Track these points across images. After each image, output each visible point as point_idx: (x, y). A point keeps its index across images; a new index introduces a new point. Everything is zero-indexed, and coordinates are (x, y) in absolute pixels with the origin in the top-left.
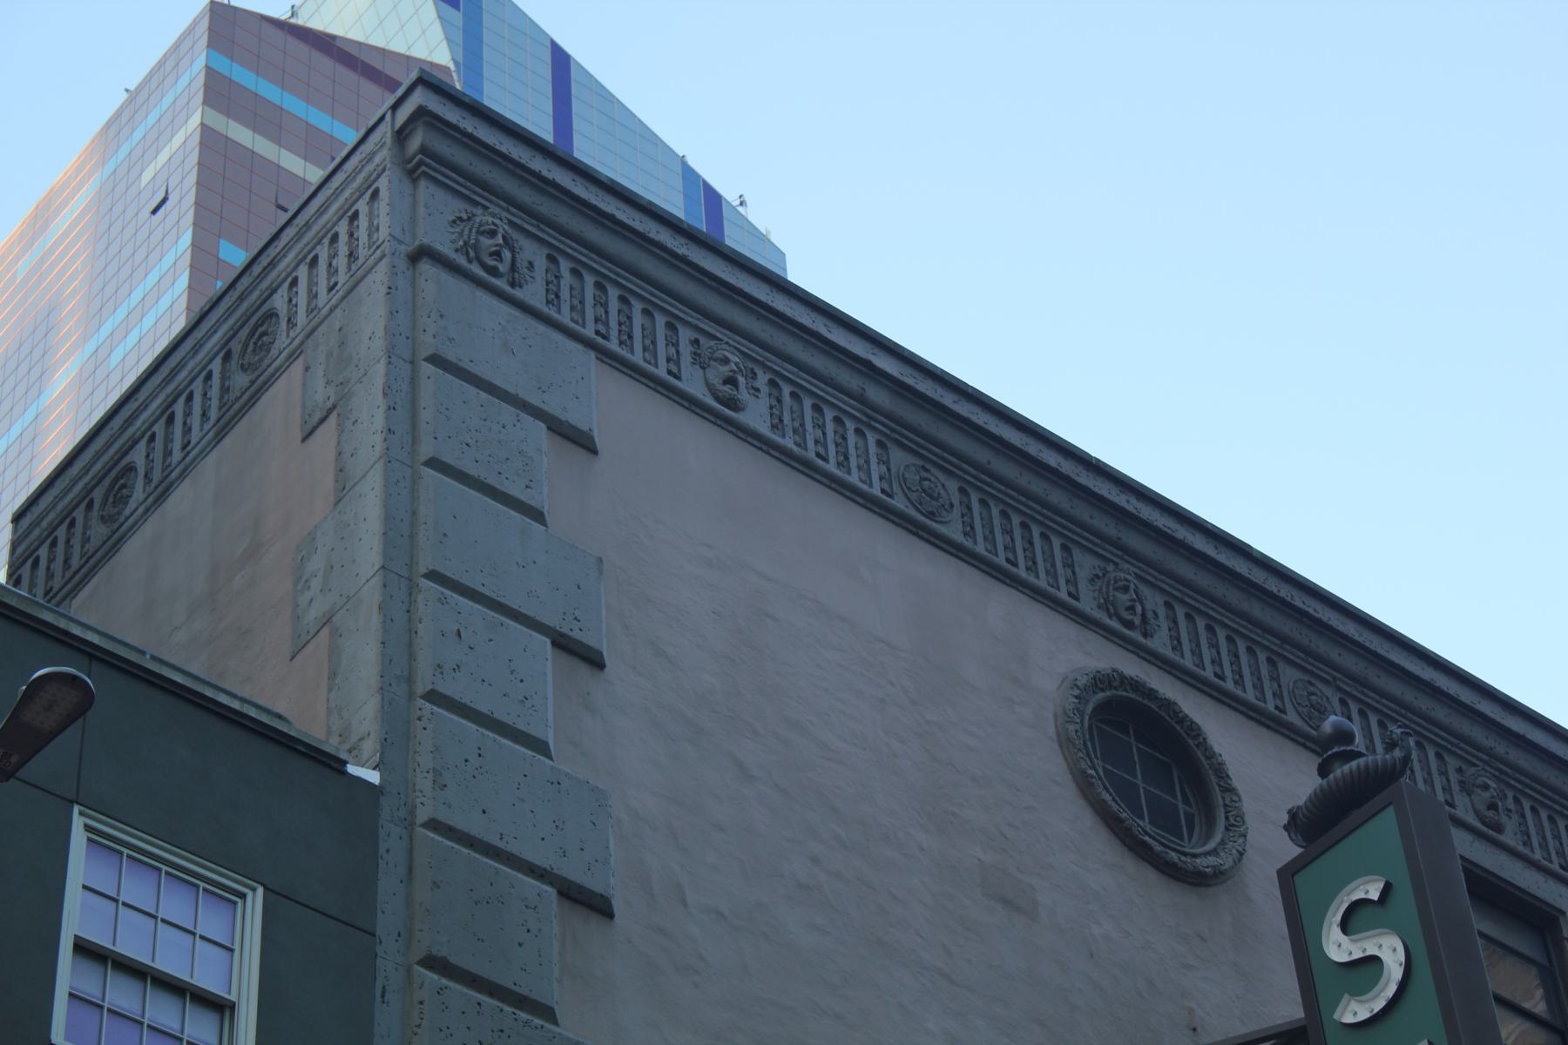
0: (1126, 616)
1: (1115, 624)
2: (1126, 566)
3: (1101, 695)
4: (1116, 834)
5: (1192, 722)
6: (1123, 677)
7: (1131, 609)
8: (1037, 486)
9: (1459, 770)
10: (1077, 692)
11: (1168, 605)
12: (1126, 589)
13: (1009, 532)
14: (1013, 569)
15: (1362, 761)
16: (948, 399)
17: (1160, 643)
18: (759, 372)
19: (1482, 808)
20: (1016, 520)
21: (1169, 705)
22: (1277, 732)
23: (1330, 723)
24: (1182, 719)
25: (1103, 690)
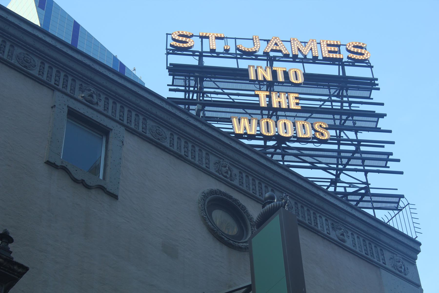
0: (225, 174)
1: (221, 176)
2: (226, 160)
3: (213, 196)
4: (215, 237)
5: (243, 206)
6: (220, 192)
7: (227, 172)
8: (197, 134)
9: (332, 224)
10: (204, 194)
11: (240, 173)
12: (225, 167)
13: (254, 185)
14: (187, 158)
15: (272, 204)
16: (97, 67)
17: (236, 183)
18: (101, 94)
19: (339, 235)
20: (257, 182)
21: (236, 200)
22: (210, 175)
23: (267, 195)
24: (240, 205)
25: (213, 195)
